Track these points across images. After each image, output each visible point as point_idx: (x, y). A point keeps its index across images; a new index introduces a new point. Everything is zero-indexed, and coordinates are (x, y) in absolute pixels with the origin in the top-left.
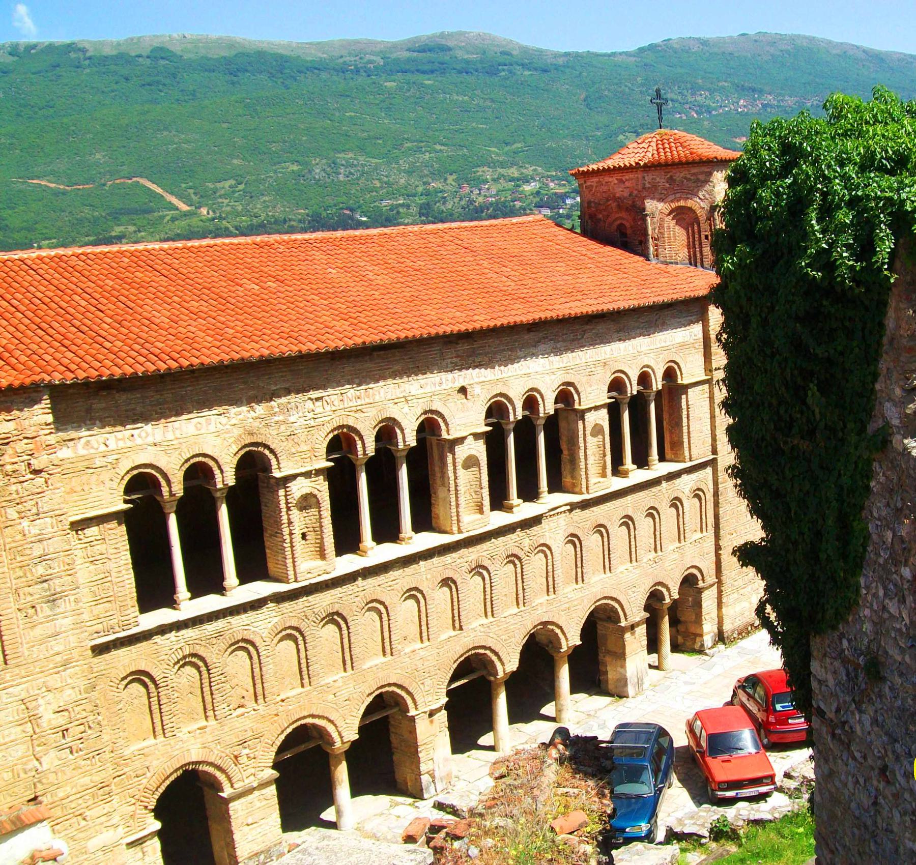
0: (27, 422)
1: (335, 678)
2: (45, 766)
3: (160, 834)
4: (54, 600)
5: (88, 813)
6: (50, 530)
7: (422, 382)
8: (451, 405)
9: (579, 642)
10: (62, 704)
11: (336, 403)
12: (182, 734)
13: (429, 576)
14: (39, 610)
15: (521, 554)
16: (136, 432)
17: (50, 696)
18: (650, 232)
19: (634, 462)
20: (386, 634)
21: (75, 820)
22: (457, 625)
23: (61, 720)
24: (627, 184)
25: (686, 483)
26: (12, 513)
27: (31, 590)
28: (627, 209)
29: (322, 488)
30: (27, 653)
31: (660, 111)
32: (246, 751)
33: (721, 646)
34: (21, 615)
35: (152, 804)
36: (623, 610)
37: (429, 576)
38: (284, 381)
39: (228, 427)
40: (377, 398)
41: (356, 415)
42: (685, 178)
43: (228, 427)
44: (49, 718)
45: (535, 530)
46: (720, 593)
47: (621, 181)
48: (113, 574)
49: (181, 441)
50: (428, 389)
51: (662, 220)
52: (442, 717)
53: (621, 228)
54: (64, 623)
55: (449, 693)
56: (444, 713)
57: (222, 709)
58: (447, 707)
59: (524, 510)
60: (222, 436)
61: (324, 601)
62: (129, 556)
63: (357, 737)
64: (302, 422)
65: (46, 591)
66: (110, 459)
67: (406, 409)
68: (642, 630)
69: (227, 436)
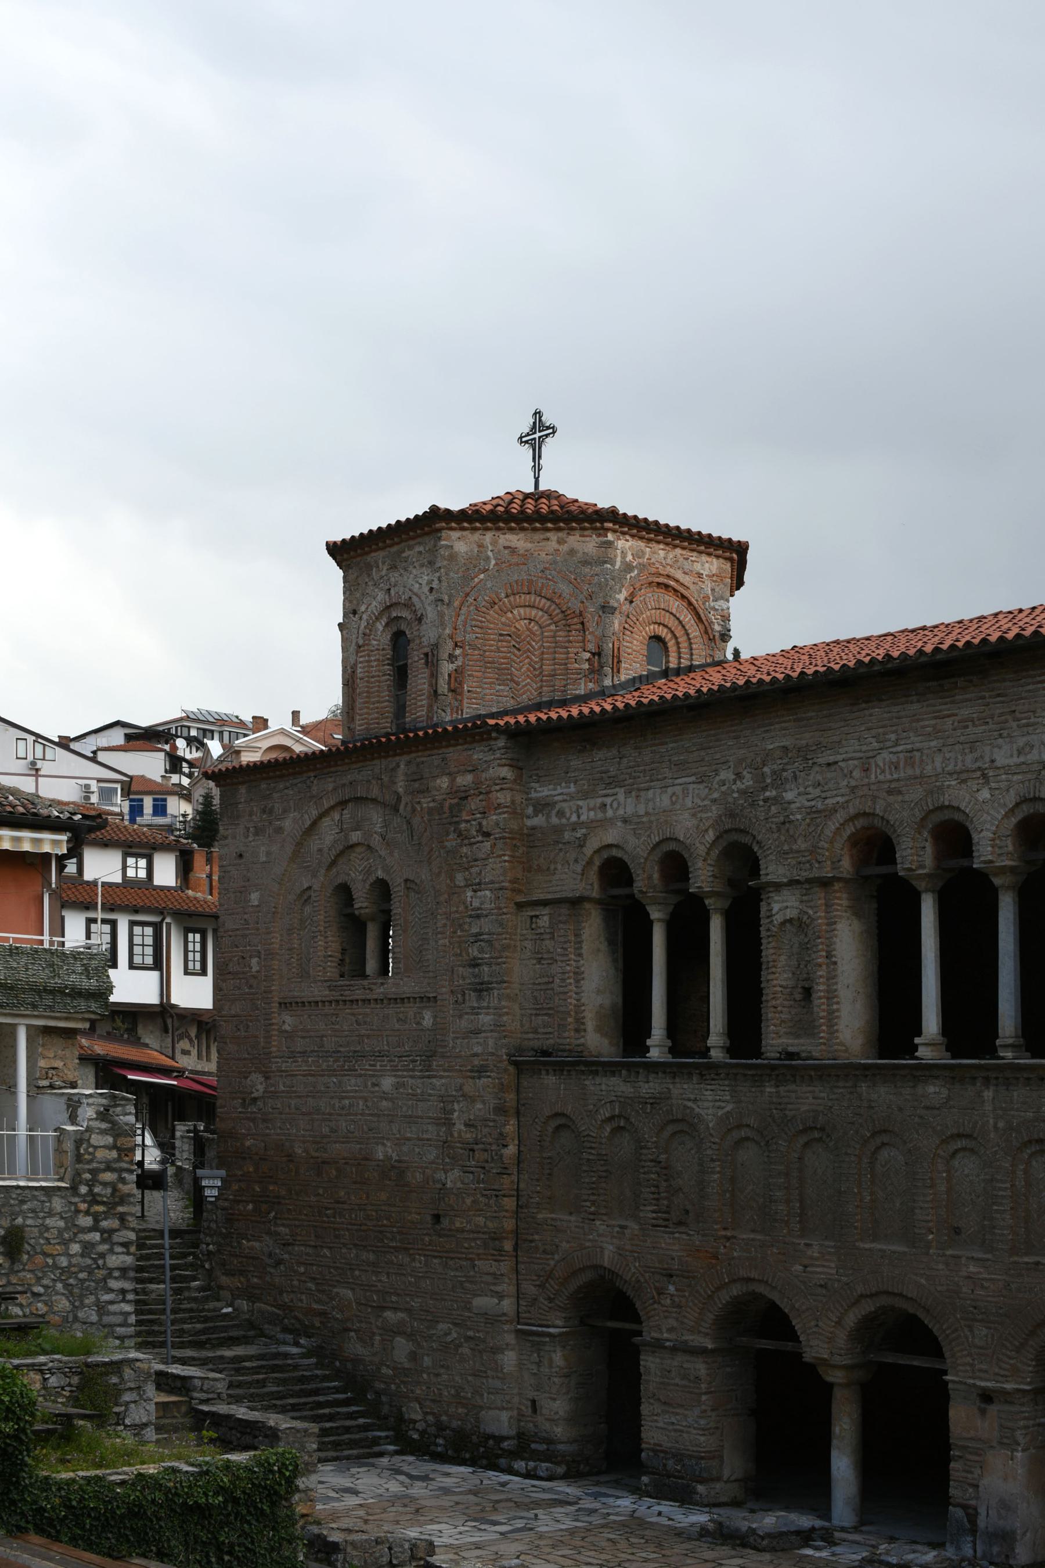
4: (481, 991)
10: (472, 1117)
11: (856, 774)
13: (1001, 1125)
14: (467, 997)
16: (608, 800)
23: (468, 1136)
37: (1001, 1124)
38: (784, 736)
39: (706, 802)
43: (706, 802)
49: (653, 818)
54: (486, 1019)
60: (699, 815)
64: (802, 801)
69: (705, 815)
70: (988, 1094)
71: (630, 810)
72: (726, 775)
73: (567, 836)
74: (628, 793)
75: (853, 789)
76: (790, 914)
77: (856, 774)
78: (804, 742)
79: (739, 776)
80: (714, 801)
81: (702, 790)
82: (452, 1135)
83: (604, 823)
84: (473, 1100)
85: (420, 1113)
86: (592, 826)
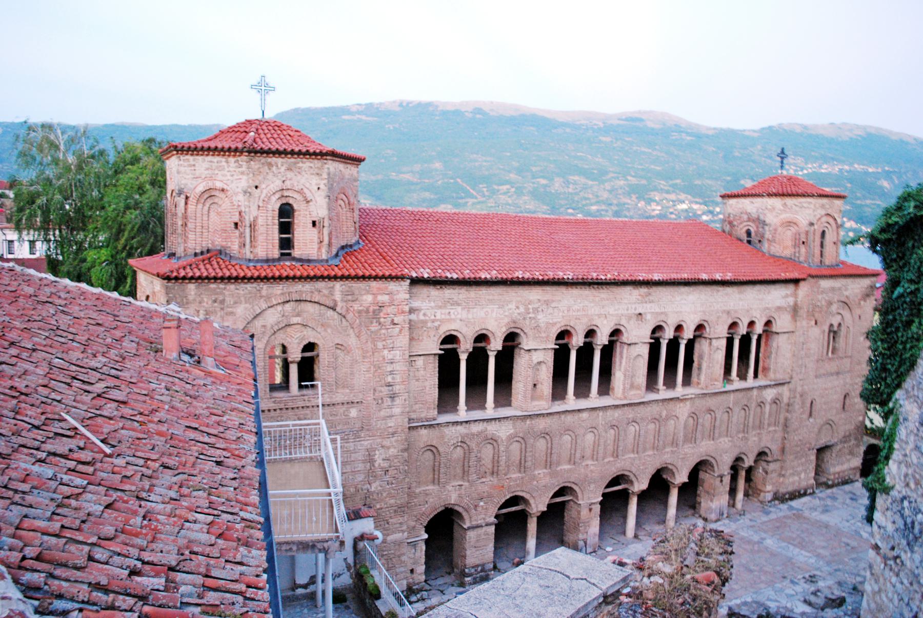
0: (395, 297)
1: (540, 472)
2: (373, 489)
3: (427, 542)
5: (391, 520)
6: (398, 357)
7: (617, 307)
8: (632, 322)
9: (687, 480)
12: (449, 488)
15: (661, 420)
16: (452, 311)
17: (383, 450)
18: (766, 236)
19: (738, 376)
20: (573, 452)
21: (383, 523)
22: (615, 455)
24: (756, 205)
25: (769, 394)
26: (380, 345)
27: (382, 389)
28: (753, 221)
29: (550, 358)
30: (374, 424)
31: (782, 162)
32: (482, 504)
33: (777, 502)
34: (375, 403)
35: (425, 524)
36: (717, 465)
40: (589, 313)
41: (577, 321)
42: (796, 205)
44: (379, 461)
45: (671, 405)
46: (782, 468)
47: (752, 203)
48: (427, 389)
50: (620, 312)
51: (776, 230)
52: (597, 508)
53: (749, 233)
54: (397, 411)
55: (604, 495)
56: (599, 507)
57: (473, 477)
58: (601, 503)
59: (663, 393)
61: (541, 424)
62: (437, 380)
63: (545, 509)
65: (390, 391)
66: (436, 324)
67: (605, 322)
68: (727, 480)
70: (601, 414)
71: (464, 314)
72: (512, 306)
73: (429, 325)
74: (463, 309)
75: (563, 317)
76: (540, 360)
77: (566, 312)
78: (545, 299)
79: (518, 307)
80: (506, 316)
81: (501, 311)
82: (373, 465)
83: (450, 320)
84: (388, 448)
85: (352, 459)
86: (442, 321)
